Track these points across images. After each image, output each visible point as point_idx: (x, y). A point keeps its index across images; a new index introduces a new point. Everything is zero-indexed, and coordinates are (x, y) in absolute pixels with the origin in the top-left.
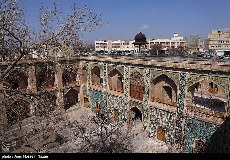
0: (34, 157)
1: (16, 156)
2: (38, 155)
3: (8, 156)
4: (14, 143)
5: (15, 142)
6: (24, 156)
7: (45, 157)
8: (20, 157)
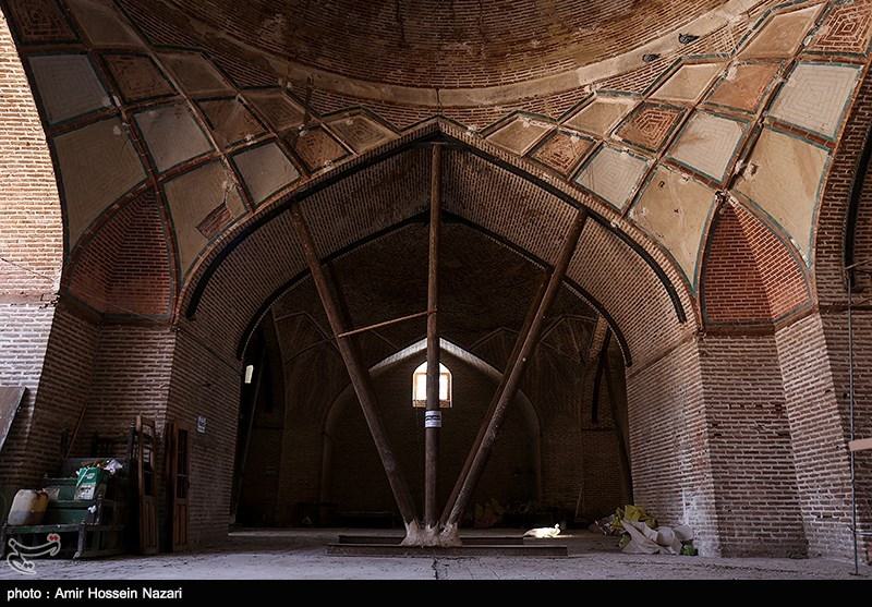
0: (131, 594)
1: (59, 592)
2: (145, 590)
3: (32, 591)
4: (54, 541)
5: (56, 538)
6: (93, 590)
7: (172, 594)
8: (77, 594)
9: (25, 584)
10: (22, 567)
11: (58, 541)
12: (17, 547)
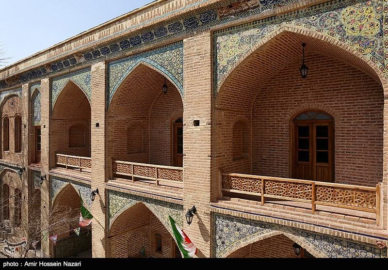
1: (26, 263)
2: (64, 262)
3: (14, 263)
7: (76, 264)
8: (34, 264)
9: (11, 260)
10: (11, 253)
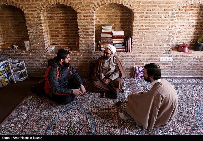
0: (30, 138)
1: (14, 138)
2: (34, 137)
3: (7, 137)
4: (13, 126)
6: (22, 137)
7: (40, 138)
8: (18, 138)
10: (5, 132)
11: (14, 126)
12: (4, 127)
